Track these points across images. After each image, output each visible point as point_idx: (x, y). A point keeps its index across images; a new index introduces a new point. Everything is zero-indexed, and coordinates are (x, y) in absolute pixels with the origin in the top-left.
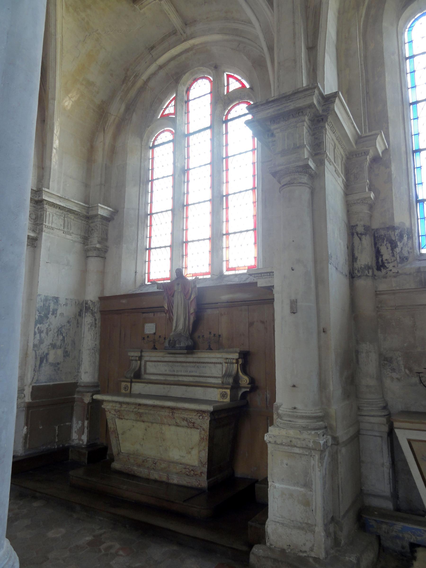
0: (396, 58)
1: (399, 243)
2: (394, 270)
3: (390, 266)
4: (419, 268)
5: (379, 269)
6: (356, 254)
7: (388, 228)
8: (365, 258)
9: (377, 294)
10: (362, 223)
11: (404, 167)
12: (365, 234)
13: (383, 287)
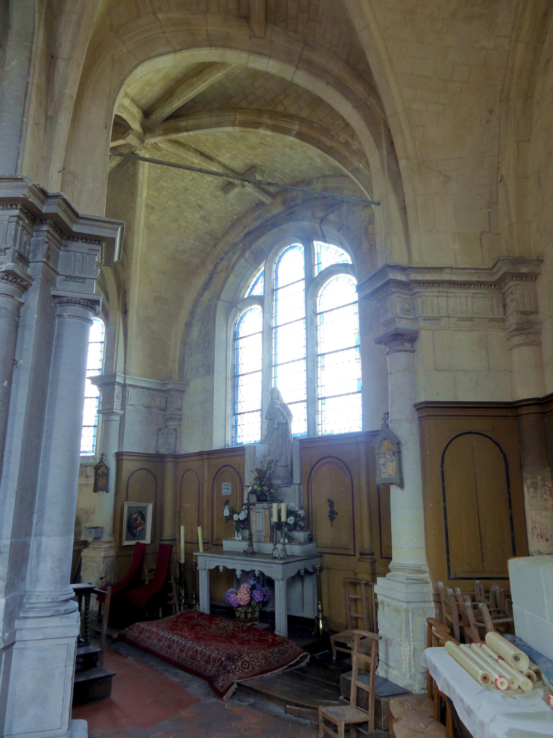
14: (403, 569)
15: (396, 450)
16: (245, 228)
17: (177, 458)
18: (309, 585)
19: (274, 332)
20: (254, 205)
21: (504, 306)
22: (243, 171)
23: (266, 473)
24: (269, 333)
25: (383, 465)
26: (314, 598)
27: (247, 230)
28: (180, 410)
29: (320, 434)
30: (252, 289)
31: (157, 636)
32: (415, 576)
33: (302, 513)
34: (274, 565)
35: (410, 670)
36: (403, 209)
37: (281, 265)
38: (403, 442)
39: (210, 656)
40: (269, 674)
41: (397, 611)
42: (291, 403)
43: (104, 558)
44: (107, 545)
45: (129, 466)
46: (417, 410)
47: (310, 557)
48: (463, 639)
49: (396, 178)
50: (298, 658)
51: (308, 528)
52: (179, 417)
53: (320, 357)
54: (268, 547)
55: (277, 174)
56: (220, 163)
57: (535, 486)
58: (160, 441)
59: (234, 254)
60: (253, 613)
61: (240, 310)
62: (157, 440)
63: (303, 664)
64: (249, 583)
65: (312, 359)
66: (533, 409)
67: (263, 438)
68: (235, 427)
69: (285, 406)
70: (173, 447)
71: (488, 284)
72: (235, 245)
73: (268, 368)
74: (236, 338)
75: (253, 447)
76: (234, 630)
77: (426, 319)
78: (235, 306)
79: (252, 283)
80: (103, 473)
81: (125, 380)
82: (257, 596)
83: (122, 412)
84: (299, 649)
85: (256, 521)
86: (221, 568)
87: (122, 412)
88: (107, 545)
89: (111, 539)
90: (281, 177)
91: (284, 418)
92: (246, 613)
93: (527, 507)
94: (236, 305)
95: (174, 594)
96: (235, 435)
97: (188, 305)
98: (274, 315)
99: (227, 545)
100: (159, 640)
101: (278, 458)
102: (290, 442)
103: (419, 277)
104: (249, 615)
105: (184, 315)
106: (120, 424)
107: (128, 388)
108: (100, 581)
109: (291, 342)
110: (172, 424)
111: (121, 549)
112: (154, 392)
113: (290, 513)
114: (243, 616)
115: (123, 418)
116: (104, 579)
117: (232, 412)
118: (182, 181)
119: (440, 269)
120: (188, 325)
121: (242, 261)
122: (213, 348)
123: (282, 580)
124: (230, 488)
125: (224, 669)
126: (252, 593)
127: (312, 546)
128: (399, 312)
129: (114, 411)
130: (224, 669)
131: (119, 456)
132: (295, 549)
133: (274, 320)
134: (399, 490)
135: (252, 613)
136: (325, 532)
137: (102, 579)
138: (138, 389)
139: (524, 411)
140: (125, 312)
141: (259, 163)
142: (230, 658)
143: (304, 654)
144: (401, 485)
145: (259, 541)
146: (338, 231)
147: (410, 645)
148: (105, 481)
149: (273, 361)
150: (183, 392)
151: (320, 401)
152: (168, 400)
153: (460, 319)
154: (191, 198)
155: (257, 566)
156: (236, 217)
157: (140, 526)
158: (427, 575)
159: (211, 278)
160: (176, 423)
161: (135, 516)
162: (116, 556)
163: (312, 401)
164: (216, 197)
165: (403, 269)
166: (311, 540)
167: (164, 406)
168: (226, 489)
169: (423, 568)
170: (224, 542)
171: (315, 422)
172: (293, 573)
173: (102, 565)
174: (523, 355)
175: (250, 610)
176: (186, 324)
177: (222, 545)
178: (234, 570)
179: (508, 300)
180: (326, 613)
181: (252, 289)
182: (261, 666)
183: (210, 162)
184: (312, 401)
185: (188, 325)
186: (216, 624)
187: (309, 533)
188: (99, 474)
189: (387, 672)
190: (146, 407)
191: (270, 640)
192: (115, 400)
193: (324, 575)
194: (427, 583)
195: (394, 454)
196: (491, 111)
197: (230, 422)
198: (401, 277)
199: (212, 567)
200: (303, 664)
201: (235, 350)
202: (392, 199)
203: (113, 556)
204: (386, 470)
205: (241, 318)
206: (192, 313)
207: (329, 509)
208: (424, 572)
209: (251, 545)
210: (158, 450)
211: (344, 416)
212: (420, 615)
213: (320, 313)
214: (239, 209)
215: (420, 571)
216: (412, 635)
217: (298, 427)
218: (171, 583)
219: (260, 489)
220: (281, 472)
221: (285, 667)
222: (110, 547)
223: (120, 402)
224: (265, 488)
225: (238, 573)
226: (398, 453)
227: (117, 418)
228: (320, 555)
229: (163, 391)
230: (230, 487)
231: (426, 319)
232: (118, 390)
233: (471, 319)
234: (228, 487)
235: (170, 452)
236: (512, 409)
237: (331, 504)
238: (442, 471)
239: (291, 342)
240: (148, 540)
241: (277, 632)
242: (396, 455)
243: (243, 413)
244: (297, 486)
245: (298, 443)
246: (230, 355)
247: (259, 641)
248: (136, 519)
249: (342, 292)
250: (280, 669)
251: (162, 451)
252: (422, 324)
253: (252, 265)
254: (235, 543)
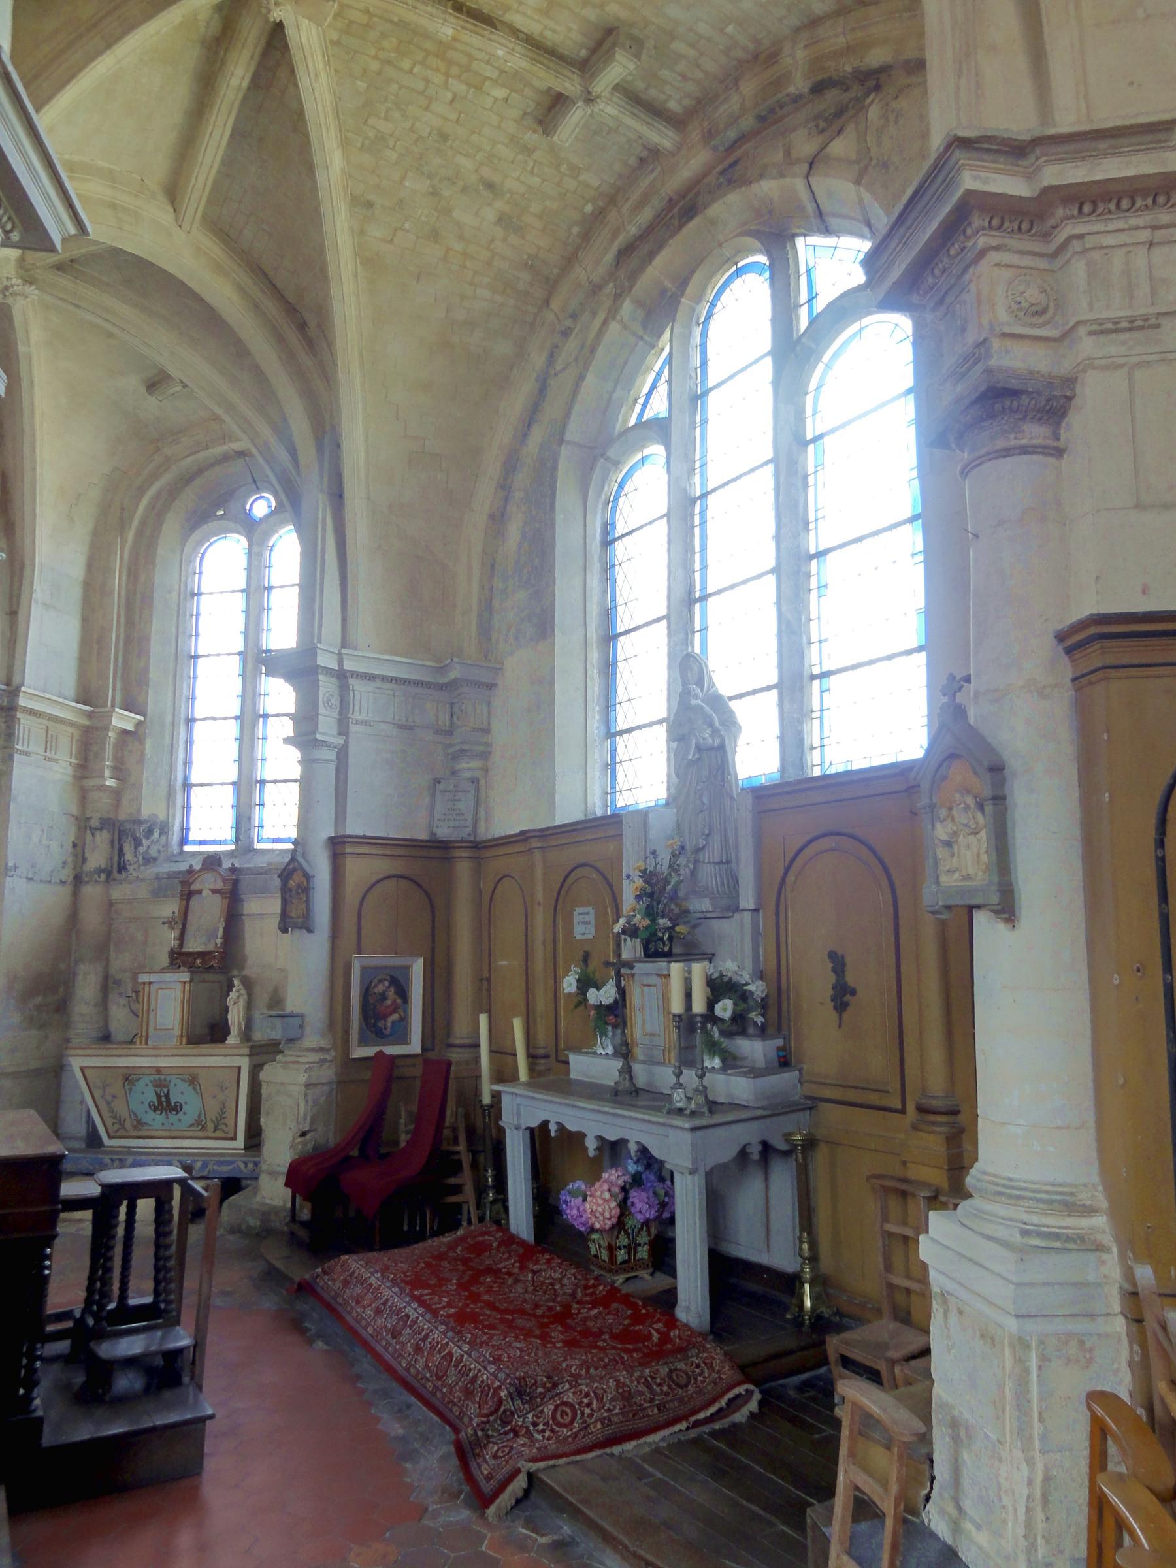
0: (175, 595)
1: (144, 841)
2: (135, 874)
3: (131, 868)
4: (158, 874)
5: (119, 872)
6: (87, 855)
7: (134, 822)
8: (97, 857)
9: (111, 904)
10: (98, 815)
11: (167, 741)
12: (101, 829)
13: (116, 894)
14: (1010, 1196)
15: (987, 792)
16: (615, 235)
17: (479, 848)
18: (783, 1179)
19: (697, 510)
20: (633, 161)
22: (583, 53)
23: (667, 882)
24: (686, 513)
25: (948, 844)
26: (794, 1218)
27: (621, 240)
28: (487, 731)
29: (817, 772)
30: (644, 406)
31: (376, 1298)
32: (1054, 1222)
33: (757, 989)
34: (671, 1132)
35: (1032, 1547)
37: (713, 325)
38: (1014, 764)
39: (475, 1377)
40: (629, 1446)
42: (741, 696)
43: (307, 1085)
44: (314, 1057)
45: (359, 870)
46: (1069, 651)
47: (778, 1108)
50: (723, 1402)
51: (779, 1028)
52: (481, 748)
53: (814, 562)
54: (664, 1077)
55: (678, 46)
56: (514, 32)
58: (439, 809)
59: (594, 314)
60: (631, 1248)
61: (617, 464)
62: (432, 807)
63: (740, 1416)
64: (626, 1169)
65: (795, 568)
67: (673, 791)
68: (611, 767)
69: (718, 703)
70: (469, 823)
72: (596, 289)
73: (686, 604)
74: (608, 540)
75: (643, 816)
76: (573, 1295)
77: (1106, 329)
78: (602, 455)
79: (645, 390)
80: (299, 886)
81: (340, 662)
82: (639, 1205)
83: (340, 741)
84: (728, 1373)
85: (642, 1009)
86: (553, 1128)
87: (340, 741)
88: (314, 1057)
89: (323, 1043)
90: (692, 53)
91: (715, 732)
92: (611, 1249)
94: (604, 453)
95: (466, 1179)
96: (611, 790)
97: (492, 467)
98: (697, 465)
99: (581, 1066)
100: (378, 1312)
101: (702, 843)
102: (732, 798)
103: (1076, 173)
104: (621, 1255)
105: (485, 495)
106: (337, 769)
107: (351, 681)
108: (299, 1140)
109: (740, 533)
110: (468, 766)
111: (349, 1064)
112: (419, 690)
113: (718, 988)
114: (604, 1255)
115: (342, 754)
116: (308, 1137)
117: (603, 730)
118: (427, 109)
120: (498, 519)
121: (614, 327)
122: (552, 570)
123: (693, 1172)
124: (593, 922)
125: (505, 1423)
126: (625, 1200)
127: (788, 1078)
128: (1003, 315)
129: (318, 737)
130: (505, 1423)
131: (337, 846)
132: (737, 1088)
133: (697, 479)
134: (1001, 927)
135: (628, 1247)
136: (823, 1042)
137: (303, 1134)
138: (378, 683)
140: (337, 496)
141: (624, 14)
142: (521, 1392)
143: (741, 1389)
144: (1007, 911)
145: (651, 1061)
146: (858, 182)
147: (1030, 1462)
148: (304, 906)
149: (698, 587)
150: (491, 686)
151: (816, 683)
152: (456, 709)
154: (461, 160)
155: (633, 1128)
156: (589, 208)
157: (394, 1011)
158: (1100, 1221)
159: (542, 390)
160: (475, 764)
161: (380, 988)
162: (339, 1082)
163: (795, 684)
164: (528, 150)
165: (1016, 150)
166: (784, 1061)
167: (448, 723)
168: (583, 925)
169: (1084, 1197)
170: (573, 1058)
171: (802, 740)
172: (728, 1154)
173: (302, 1104)
175: (624, 1240)
176: (492, 517)
177: (568, 1063)
178: (581, 1136)
180: (826, 1265)
181: (644, 406)
182: (606, 1422)
183: (487, 31)
184: (795, 684)
185: (498, 519)
186: (534, 1272)
187: (780, 1042)
188: (291, 890)
189: (956, 1528)
190: (400, 727)
191: (656, 1337)
192: (321, 710)
193: (820, 1157)
194: (1099, 1248)
195: (981, 807)
197: (597, 756)
198: (1007, 183)
199: (534, 1124)
200: (740, 1416)
201: (608, 570)
203: (330, 1083)
204: (960, 863)
205: (621, 486)
206: (505, 487)
207: (832, 978)
208: (1089, 1211)
209: (627, 1070)
210: (435, 829)
211: (879, 721)
212: (1069, 1361)
213: (815, 439)
214: (595, 182)
215: (1071, 1207)
216: (1037, 1429)
217: (756, 759)
218: (458, 1153)
219: (647, 922)
220: (709, 875)
221: (683, 1426)
222: (323, 1061)
223: (336, 715)
224: (662, 922)
225: (591, 1144)
227: (332, 755)
228: (811, 1104)
229: (442, 687)
230: (591, 918)
231: (1106, 329)
232: (327, 687)
234: (587, 918)
235: (463, 834)
237: (838, 963)
238: (1161, 863)
239: (740, 533)
240: (415, 1046)
241: (681, 1314)
242: (989, 808)
243: (629, 730)
244: (747, 917)
245: (749, 800)
246: (594, 582)
247: (625, 1336)
248: (383, 997)
249: (878, 368)
250: (666, 1432)
251: (444, 832)
252: (1087, 346)
253: (641, 338)
254: (595, 1065)
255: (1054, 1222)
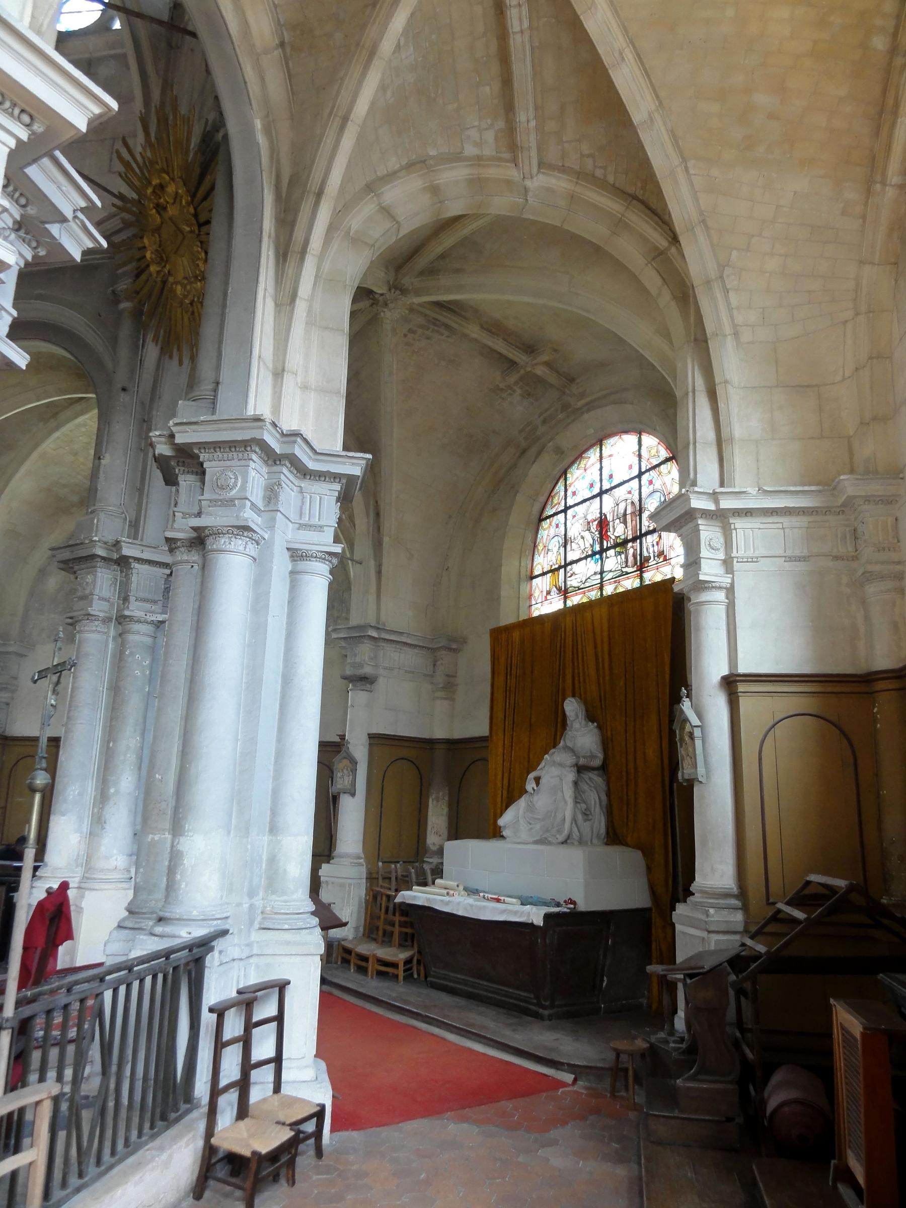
21: (434, 665)
28: (16, 678)
32: (356, 861)
36: (379, 573)
41: (342, 886)
48: (425, 884)
49: (378, 545)
57: (437, 799)
66: (442, 746)
71: (428, 649)
77: (385, 668)
93: (430, 813)
103: (387, 637)
119: (401, 633)
139: (437, 746)
144: (353, 795)
153: (406, 671)
158: (362, 861)
174: (441, 706)
176: (40, 571)
179: (439, 663)
196: (450, 517)
202: (372, 563)
215: (359, 858)
226: (354, 771)
231: (385, 668)
233: (413, 673)
236: (429, 744)
252: (381, 671)
255: (356, 861)
